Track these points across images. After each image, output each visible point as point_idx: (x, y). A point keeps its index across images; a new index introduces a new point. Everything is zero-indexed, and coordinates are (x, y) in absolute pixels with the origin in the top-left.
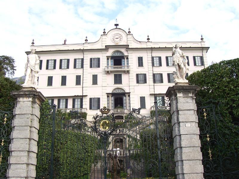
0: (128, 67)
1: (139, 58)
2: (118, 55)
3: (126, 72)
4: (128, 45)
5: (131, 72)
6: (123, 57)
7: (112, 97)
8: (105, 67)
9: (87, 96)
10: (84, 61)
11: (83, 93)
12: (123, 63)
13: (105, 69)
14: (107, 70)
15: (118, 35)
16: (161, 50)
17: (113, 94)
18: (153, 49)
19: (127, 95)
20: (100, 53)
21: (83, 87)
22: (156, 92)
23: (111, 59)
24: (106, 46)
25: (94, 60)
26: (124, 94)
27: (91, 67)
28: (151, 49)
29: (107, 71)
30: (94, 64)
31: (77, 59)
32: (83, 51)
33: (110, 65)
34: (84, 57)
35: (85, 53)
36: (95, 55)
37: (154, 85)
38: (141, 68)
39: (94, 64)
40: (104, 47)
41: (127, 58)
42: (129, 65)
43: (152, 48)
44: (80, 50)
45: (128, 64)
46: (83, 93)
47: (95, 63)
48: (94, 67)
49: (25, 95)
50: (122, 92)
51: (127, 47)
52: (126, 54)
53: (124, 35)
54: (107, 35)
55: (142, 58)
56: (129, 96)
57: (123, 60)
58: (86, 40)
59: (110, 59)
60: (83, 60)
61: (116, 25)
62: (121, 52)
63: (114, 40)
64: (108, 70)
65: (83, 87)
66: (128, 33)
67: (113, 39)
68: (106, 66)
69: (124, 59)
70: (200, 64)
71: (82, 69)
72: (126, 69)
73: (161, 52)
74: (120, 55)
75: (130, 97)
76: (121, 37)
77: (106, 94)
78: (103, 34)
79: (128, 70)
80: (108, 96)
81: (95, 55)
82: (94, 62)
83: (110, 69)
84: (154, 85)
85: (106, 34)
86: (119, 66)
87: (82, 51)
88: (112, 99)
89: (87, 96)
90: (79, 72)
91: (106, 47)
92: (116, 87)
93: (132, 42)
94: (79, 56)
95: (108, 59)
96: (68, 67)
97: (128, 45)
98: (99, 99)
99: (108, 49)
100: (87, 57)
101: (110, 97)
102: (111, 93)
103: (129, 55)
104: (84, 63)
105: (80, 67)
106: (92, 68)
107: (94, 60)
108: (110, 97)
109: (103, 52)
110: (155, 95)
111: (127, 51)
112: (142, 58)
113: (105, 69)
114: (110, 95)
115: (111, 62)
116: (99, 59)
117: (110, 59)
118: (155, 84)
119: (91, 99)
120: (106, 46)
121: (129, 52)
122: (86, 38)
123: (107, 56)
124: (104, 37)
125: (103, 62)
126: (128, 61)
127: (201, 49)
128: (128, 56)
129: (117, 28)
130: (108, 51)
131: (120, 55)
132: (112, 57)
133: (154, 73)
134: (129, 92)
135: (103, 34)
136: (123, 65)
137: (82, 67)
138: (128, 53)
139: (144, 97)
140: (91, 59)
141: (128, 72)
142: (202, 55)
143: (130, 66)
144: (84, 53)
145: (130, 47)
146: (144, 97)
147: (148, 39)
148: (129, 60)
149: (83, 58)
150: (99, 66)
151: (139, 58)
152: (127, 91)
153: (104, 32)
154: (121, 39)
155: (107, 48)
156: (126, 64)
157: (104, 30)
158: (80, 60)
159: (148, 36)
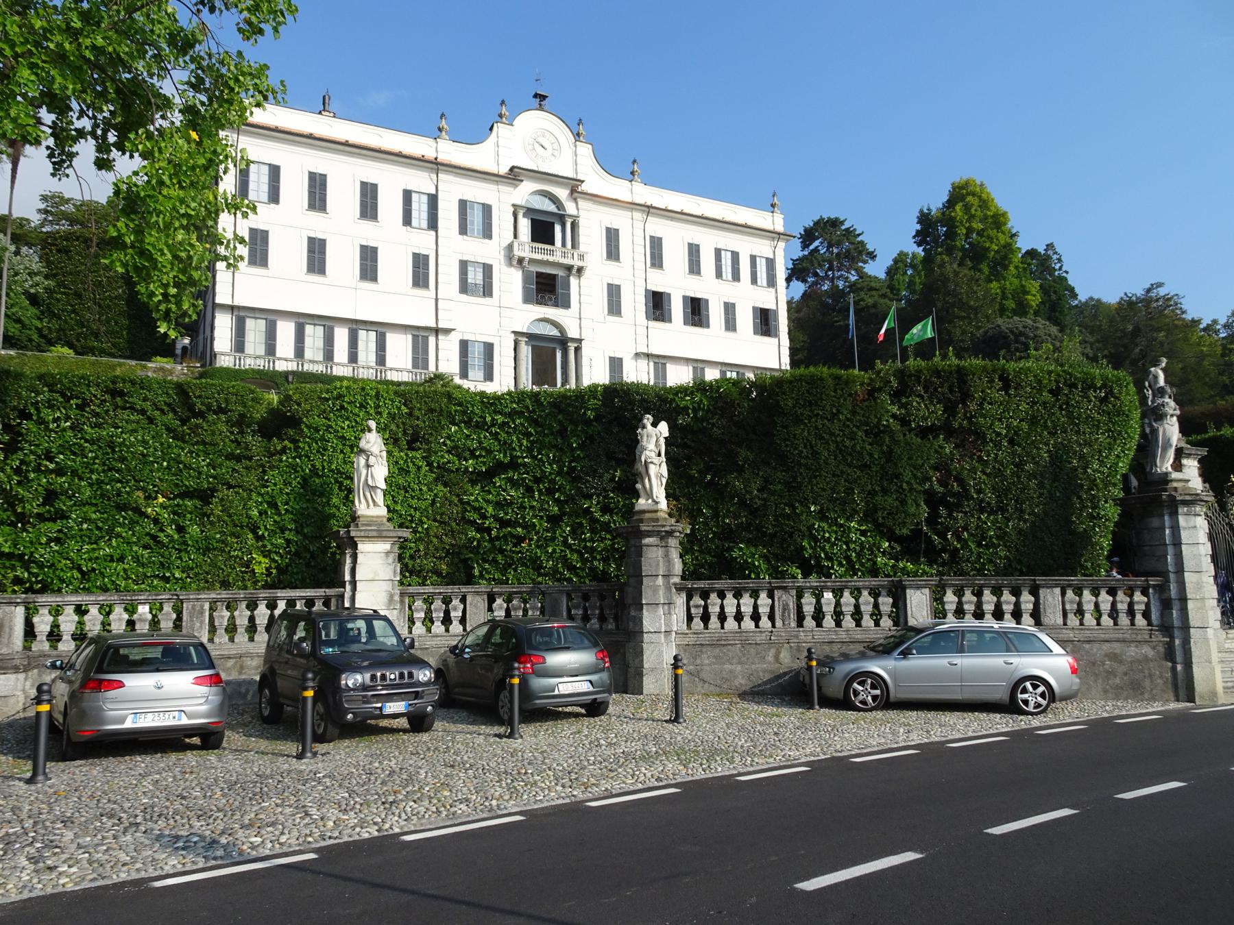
5: (587, 274)
6: (562, 219)
15: (547, 134)
16: (672, 219)
18: (651, 210)
19: (572, 346)
20: (493, 187)
21: (437, 300)
26: (563, 341)
32: (440, 167)
36: (478, 192)
40: (504, 170)
43: (651, 207)
47: (476, 218)
50: (555, 332)
52: (570, 208)
60: (433, 200)
62: (554, 199)
70: (765, 283)
72: (576, 263)
79: (580, 264)
80: (516, 343)
81: (478, 192)
88: (526, 351)
90: (422, 241)
94: (421, 182)
100: (452, 190)
109: (503, 188)
111: (575, 200)
118: (652, 324)
119: (464, 345)
123: (513, 205)
127: (773, 239)
130: (516, 186)
131: (552, 208)
134: (577, 337)
137: (433, 224)
139: (621, 360)
141: (580, 270)
142: (772, 257)
145: (584, 187)
148: (582, 231)
149: (434, 192)
152: (572, 333)
154: (556, 153)
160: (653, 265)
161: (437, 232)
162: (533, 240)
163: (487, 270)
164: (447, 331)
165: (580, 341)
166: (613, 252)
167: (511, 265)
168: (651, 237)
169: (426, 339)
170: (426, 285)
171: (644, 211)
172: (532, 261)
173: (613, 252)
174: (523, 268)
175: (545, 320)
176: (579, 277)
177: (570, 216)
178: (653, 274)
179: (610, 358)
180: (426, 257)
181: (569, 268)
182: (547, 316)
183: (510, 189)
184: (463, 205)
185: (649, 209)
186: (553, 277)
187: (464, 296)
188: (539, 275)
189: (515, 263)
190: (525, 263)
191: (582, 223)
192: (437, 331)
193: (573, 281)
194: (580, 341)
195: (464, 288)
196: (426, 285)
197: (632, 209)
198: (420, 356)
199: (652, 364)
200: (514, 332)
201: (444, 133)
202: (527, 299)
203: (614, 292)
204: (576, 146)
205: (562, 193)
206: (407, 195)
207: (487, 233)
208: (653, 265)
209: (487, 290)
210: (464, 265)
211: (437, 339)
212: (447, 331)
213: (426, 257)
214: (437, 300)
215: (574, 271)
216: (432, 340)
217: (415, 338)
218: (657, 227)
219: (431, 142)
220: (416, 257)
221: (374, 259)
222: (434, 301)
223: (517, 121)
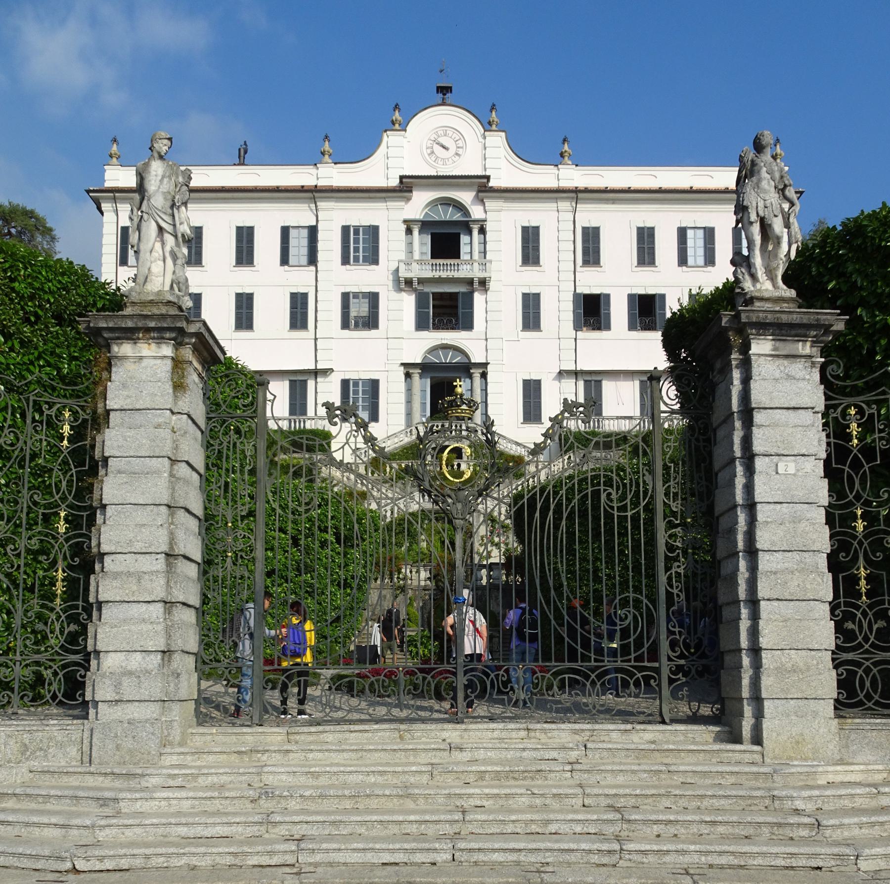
0: (484, 265)
1: (525, 230)
2: (445, 216)
4: (488, 178)
5: (492, 285)
6: (466, 225)
7: (421, 377)
8: (399, 261)
9: (332, 370)
10: (321, 236)
11: (316, 361)
12: (464, 249)
13: (397, 270)
14: (404, 274)
15: (450, 132)
16: (614, 201)
17: (425, 368)
18: (580, 195)
19: (476, 373)
20: (381, 205)
21: (316, 339)
22: (583, 366)
23: (420, 232)
24: (402, 178)
25: (357, 232)
26: (466, 368)
27: (345, 261)
28: (574, 195)
29: (405, 279)
30: (356, 250)
31: (293, 227)
32: (317, 195)
33: (417, 256)
34: (317, 221)
35: (321, 204)
37: (576, 339)
38: (530, 270)
39: (356, 250)
40: (394, 182)
41: (482, 231)
42: (489, 256)
43: (576, 191)
44: (302, 189)
45: (485, 252)
46: (316, 361)
48: (356, 259)
49: (130, 334)
52: (476, 212)
54: (405, 130)
55: (537, 229)
56: (484, 375)
57: (464, 239)
59: (416, 232)
60: (313, 232)
62: (459, 206)
63: (433, 152)
64: (409, 275)
65: (316, 339)
66: (487, 127)
67: (429, 151)
68: (403, 256)
69: (470, 232)
71: (313, 268)
72: (476, 273)
74: (455, 218)
75: (486, 379)
76: (460, 143)
77: (402, 368)
79: (482, 275)
80: (408, 375)
82: (356, 241)
83: (417, 271)
84: (576, 339)
86: (449, 261)
87: (310, 195)
88: (422, 386)
89: (333, 374)
91: (401, 182)
92: (439, 342)
93: (503, 164)
95: (409, 231)
97: (488, 178)
98: (374, 385)
101: (416, 377)
102: (419, 361)
103: (490, 216)
104: (320, 246)
105: (304, 260)
106: (348, 267)
107: (357, 232)
108: (416, 377)
110: (576, 374)
111: (482, 202)
112: (537, 229)
113: (397, 270)
114: (416, 372)
115: (422, 244)
116: (373, 232)
117: (416, 232)
119: (345, 383)
120: (402, 178)
121: (489, 204)
123: (405, 221)
126: (485, 243)
129: (444, 104)
130: (409, 199)
131: (458, 217)
132: (425, 225)
133: (577, 291)
137: (313, 259)
138: (486, 212)
139: (538, 383)
140: (345, 230)
141: (483, 283)
143: (491, 262)
144: (318, 204)
146: (538, 383)
149: (314, 223)
151: (525, 230)
152: (477, 357)
154: (460, 151)
156: (476, 256)
158: (305, 233)
160: (586, 263)
161: (316, 266)
162: (433, 257)
163: (373, 299)
164: (326, 372)
165: (485, 365)
167: (400, 290)
168: (585, 230)
169: (305, 383)
170: (304, 326)
171: (573, 198)
172: (421, 281)
174: (415, 290)
175: (445, 347)
176: (486, 290)
177: (476, 221)
179: (524, 381)
180: (305, 296)
181: (470, 282)
182: (445, 342)
185: (577, 194)
186: (453, 296)
187: (346, 332)
188: (437, 296)
189: (403, 286)
190: (415, 284)
191: (489, 227)
192: (316, 373)
193: (478, 299)
194: (485, 365)
195: (345, 325)
196: (304, 326)
197: (556, 200)
198: (298, 404)
199: (581, 384)
200: (402, 364)
201: (327, 156)
202: (421, 324)
204: (485, 138)
205: (466, 197)
206: (285, 232)
207: (373, 258)
208: (586, 263)
209: (371, 322)
210: (345, 297)
211: (316, 383)
212: (326, 372)
213: (305, 296)
215: (476, 285)
216: (311, 384)
217: (293, 384)
219: (311, 169)
220: (294, 296)
221: (250, 306)
223: (408, 129)
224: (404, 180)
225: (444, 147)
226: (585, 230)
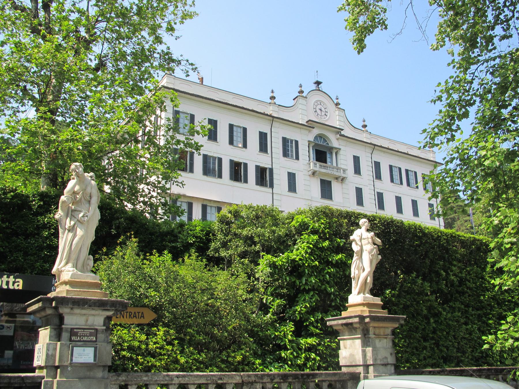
3: (340, 179)
4: (342, 130)
5: (347, 181)
6: (331, 149)
12: (328, 160)
16: (384, 152)
20: (298, 130)
21: (273, 194)
28: (373, 146)
36: (292, 134)
43: (375, 145)
51: (338, 131)
53: (331, 107)
58: (273, 98)
61: (318, 83)
63: (316, 111)
69: (331, 153)
72: (341, 174)
73: (382, 154)
78: (299, 95)
79: (344, 175)
85: (304, 95)
96: (245, 146)
99: (313, 128)
106: (285, 158)
109: (303, 131)
111: (337, 139)
122: (273, 92)
123: (309, 141)
124: (301, 101)
125: (304, 150)
128: (340, 149)
130: (310, 131)
135: (299, 95)
136: (329, 164)
141: (343, 179)
145: (343, 133)
147: (365, 126)
150: (297, 158)
153: (301, 92)
155: (310, 125)
157: (301, 86)
159: (364, 121)
160: (377, 178)
166: (357, 171)
168: (375, 162)
171: (372, 147)
173: (357, 171)
177: (336, 148)
178: (377, 182)
183: (307, 132)
184: (285, 141)
191: (341, 152)
203: (359, 192)
208: (377, 178)
214: (273, 194)
218: (378, 157)
222: (271, 195)
224: (310, 122)
225: (321, 110)
226: (375, 162)
